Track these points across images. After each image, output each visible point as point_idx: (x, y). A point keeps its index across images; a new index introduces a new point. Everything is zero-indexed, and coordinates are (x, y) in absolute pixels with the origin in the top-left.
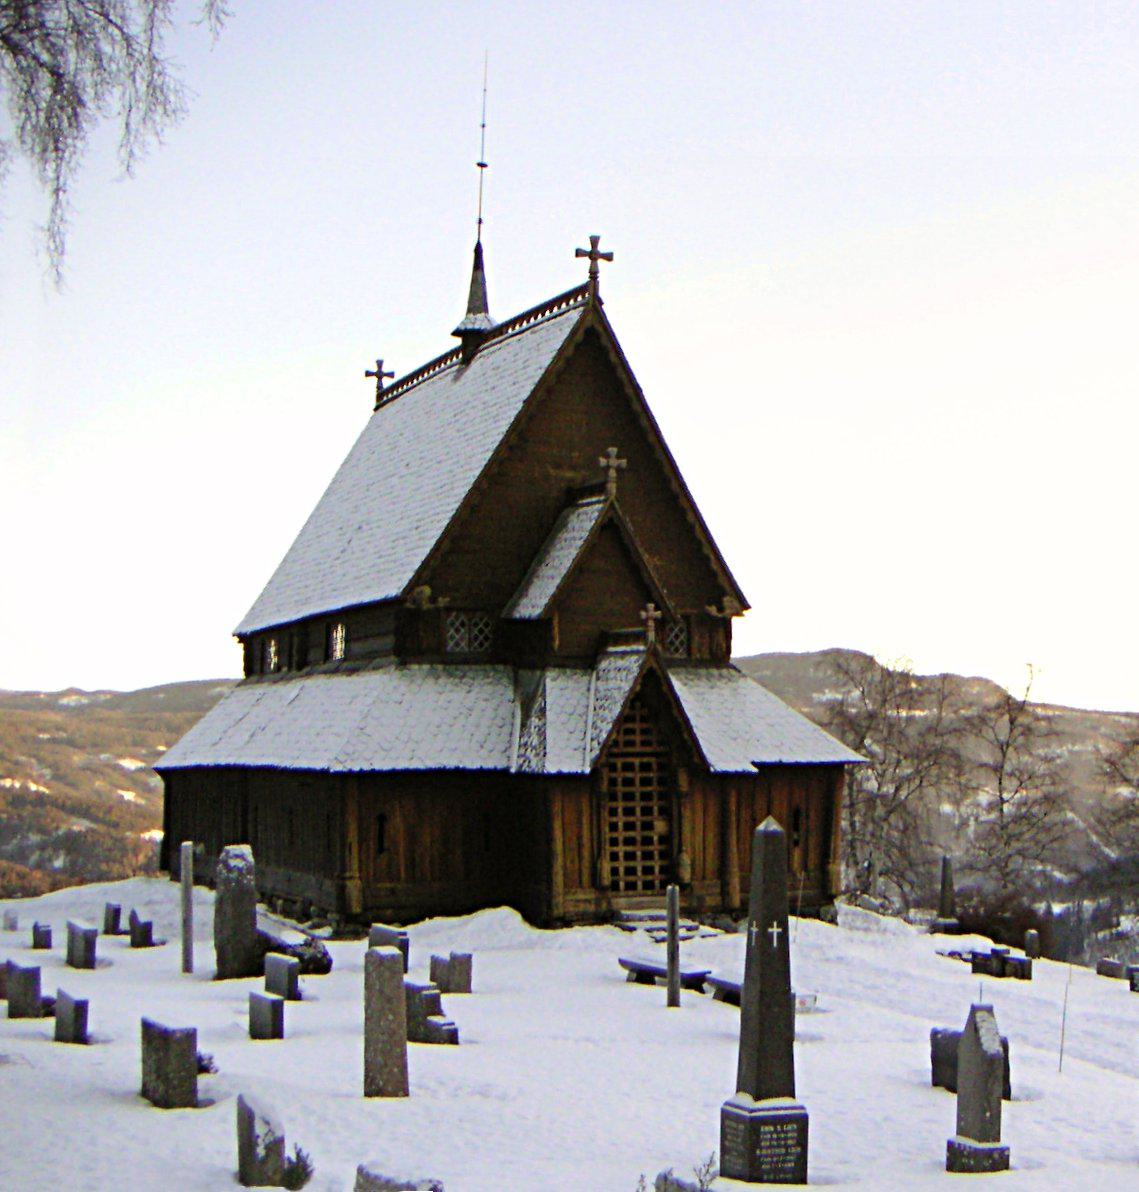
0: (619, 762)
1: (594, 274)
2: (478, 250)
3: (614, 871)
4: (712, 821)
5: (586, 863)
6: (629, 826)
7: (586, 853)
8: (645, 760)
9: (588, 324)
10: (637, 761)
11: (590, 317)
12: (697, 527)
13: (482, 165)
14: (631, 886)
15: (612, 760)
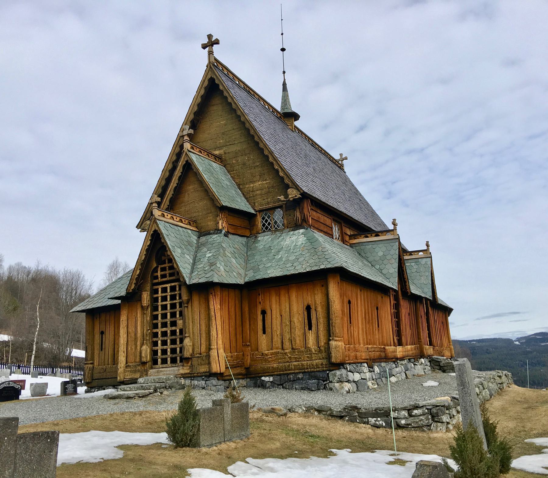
0: (160, 288)
1: (211, 53)
2: (284, 85)
3: (155, 353)
4: (203, 316)
5: (139, 348)
6: (164, 325)
7: (139, 343)
8: (173, 284)
9: (209, 77)
10: (168, 286)
11: (210, 73)
12: (270, 156)
13: (283, 50)
14: (164, 361)
15: (155, 287)
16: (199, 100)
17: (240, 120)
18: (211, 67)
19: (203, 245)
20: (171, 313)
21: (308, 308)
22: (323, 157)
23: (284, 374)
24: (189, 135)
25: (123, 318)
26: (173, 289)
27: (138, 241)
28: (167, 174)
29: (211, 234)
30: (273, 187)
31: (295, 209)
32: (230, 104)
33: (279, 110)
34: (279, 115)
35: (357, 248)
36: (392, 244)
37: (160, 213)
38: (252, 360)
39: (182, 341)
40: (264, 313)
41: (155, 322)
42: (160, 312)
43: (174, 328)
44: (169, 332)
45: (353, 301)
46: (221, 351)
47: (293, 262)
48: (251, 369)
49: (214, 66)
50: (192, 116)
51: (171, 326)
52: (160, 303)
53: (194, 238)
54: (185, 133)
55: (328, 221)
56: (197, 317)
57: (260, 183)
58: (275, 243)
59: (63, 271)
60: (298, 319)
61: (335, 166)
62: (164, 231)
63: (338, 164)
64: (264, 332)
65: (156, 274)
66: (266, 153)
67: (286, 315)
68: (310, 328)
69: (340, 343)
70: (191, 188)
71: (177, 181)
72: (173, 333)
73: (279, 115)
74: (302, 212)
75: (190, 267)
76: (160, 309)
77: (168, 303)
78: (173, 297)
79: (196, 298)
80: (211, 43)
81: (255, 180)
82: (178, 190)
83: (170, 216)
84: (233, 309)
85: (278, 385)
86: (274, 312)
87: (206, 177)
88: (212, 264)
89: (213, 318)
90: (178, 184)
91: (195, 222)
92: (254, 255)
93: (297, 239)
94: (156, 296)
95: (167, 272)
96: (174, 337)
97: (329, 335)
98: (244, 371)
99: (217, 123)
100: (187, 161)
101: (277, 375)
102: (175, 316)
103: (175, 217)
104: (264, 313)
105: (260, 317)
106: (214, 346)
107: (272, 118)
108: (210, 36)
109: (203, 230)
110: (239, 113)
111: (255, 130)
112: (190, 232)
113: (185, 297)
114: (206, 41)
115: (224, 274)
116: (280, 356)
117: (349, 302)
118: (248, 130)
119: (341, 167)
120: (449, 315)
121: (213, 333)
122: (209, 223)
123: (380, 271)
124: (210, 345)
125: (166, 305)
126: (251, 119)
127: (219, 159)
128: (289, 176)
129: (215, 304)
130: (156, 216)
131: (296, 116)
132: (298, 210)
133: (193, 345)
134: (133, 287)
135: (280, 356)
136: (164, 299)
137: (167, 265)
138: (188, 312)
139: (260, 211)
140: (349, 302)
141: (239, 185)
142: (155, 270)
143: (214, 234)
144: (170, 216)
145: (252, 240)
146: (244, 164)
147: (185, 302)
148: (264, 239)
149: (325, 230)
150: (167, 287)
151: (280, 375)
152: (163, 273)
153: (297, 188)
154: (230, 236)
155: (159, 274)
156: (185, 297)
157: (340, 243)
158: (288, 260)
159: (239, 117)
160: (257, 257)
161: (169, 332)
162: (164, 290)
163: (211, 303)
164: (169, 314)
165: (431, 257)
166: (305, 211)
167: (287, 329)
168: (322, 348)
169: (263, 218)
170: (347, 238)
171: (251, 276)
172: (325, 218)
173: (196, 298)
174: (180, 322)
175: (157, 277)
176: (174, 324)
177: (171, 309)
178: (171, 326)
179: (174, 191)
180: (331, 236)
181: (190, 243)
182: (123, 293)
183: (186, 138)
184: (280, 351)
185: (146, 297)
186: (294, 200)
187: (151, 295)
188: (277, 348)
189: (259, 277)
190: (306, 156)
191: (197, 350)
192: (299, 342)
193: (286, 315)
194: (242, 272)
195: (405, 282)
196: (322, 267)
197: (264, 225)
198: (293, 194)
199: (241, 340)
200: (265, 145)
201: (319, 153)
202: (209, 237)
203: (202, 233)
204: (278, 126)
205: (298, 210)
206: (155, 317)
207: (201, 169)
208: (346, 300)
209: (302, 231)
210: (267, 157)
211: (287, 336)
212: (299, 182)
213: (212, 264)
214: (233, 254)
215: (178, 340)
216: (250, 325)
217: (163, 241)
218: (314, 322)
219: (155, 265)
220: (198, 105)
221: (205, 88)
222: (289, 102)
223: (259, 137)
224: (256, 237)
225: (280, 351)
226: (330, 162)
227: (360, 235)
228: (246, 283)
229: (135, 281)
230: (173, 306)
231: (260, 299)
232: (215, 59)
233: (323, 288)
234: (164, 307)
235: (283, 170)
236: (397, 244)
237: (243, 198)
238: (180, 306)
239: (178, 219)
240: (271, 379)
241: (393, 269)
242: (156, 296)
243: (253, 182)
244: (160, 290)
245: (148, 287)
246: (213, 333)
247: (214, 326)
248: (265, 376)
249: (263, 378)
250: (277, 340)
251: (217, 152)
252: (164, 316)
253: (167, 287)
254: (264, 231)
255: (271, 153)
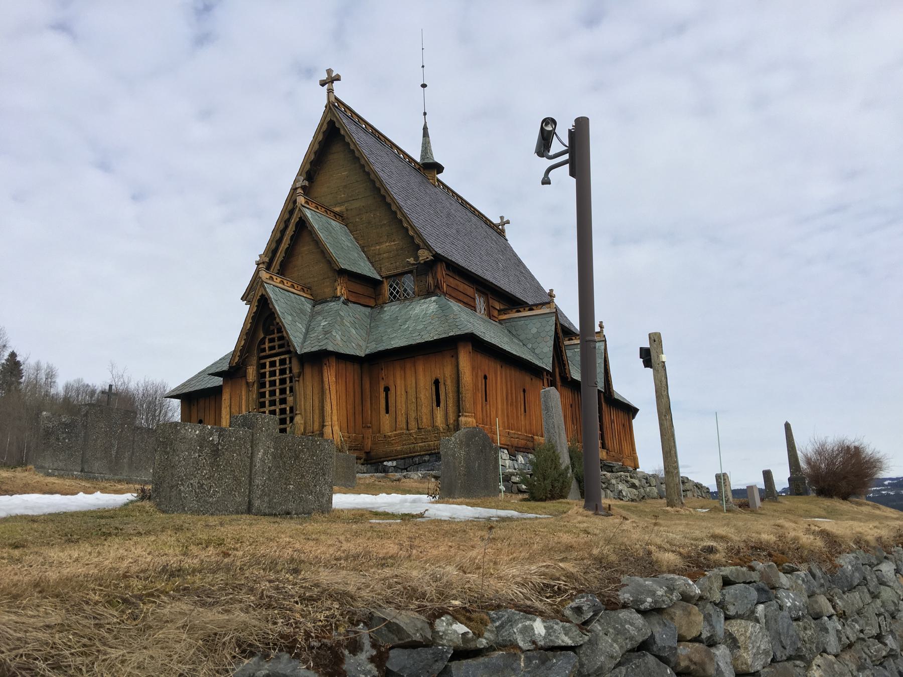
0: (267, 362)
1: (330, 91)
2: (425, 129)
4: (316, 391)
6: (273, 403)
8: (283, 357)
9: (328, 119)
10: (277, 359)
13: (424, 86)
15: (263, 361)
16: (317, 147)
17: (364, 171)
18: (330, 108)
19: (318, 313)
20: (280, 390)
21: (437, 383)
22: (474, 219)
23: (409, 457)
24: (303, 188)
25: (226, 396)
26: (283, 362)
27: (241, 312)
28: (278, 235)
29: (326, 301)
30: (402, 249)
31: (427, 274)
32: (353, 151)
33: (419, 160)
34: (417, 167)
35: (508, 324)
36: (548, 319)
37: (268, 276)
38: (374, 443)
39: (292, 419)
40: (387, 389)
41: (262, 400)
42: (268, 388)
43: (283, 406)
44: (278, 410)
45: (491, 377)
46: (336, 428)
47: (420, 331)
48: (372, 454)
49: (335, 107)
50: (308, 167)
51: (280, 404)
52: (268, 379)
53: (308, 307)
54: (298, 185)
55: (470, 290)
56: (309, 392)
57: (388, 246)
58: (403, 312)
59: (142, 382)
60: (426, 394)
61: (492, 230)
62: (271, 296)
63: (498, 230)
64: (387, 412)
65: (263, 346)
66: (394, 208)
67: (412, 392)
68: (438, 405)
69: (470, 419)
70: (305, 250)
71: (288, 242)
72: (283, 411)
73: (417, 167)
74: (435, 277)
75: (302, 337)
76: (267, 386)
77: (277, 378)
78: (283, 372)
79: (308, 371)
80: (330, 80)
81: (381, 240)
82: (290, 252)
83: (279, 279)
84: (351, 385)
85: (402, 469)
86: (398, 389)
87: (322, 235)
88: (326, 333)
89: (328, 392)
90: (290, 245)
91: (309, 288)
92: (377, 327)
93: (430, 306)
94: (263, 371)
95: (276, 343)
96: (283, 416)
97: (459, 411)
98: (364, 456)
99: (337, 174)
100: (300, 218)
101: (401, 459)
102: (285, 393)
103: (285, 282)
104: (387, 389)
105: (383, 395)
106: (328, 423)
107: (408, 169)
108: (329, 71)
109: (319, 298)
110: (363, 162)
111: (381, 182)
112: (303, 299)
113: (296, 370)
114: (324, 77)
115: (340, 343)
116: (404, 437)
117: (485, 377)
118: (373, 182)
119: (501, 233)
120: (633, 418)
121: (328, 408)
122: (326, 290)
123: (533, 350)
124: (323, 422)
125: (275, 381)
126: (377, 169)
127: (339, 216)
128: (419, 235)
129: (330, 375)
130: (264, 279)
131: (439, 168)
132: (430, 275)
133: (305, 423)
134: (236, 360)
135: (404, 437)
136: (273, 374)
137: (276, 336)
138: (299, 387)
139: (387, 278)
140: (485, 377)
141: (363, 248)
142: (263, 342)
143: (331, 301)
144: (279, 279)
145: (376, 311)
146: (369, 223)
147: (296, 375)
148: (391, 310)
149: (465, 300)
150: (275, 361)
151: (404, 458)
152: (271, 344)
153: (429, 248)
154: (350, 305)
155: (267, 345)
156: (296, 370)
157: (487, 318)
158: (415, 330)
159: (363, 166)
160: (381, 329)
161: (278, 410)
162: (273, 364)
163: (325, 375)
164: (278, 391)
165: (605, 341)
166: (439, 276)
167: (413, 407)
168: (451, 426)
169: (391, 286)
170: (496, 313)
171: (373, 348)
172: (466, 287)
173: (308, 371)
174: (290, 399)
175: (264, 350)
176: (283, 401)
177: (280, 384)
178: (280, 404)
179: (286, 253)
180: (474, 308)
181: (302, 312)
182: (225, 367)
183: (299, 191)
184: (405, 431)
185: (251, 373)
186: (425, 262)
187: (258, 371)
188: (401, 429)
189: (382, 347)
190: (449, 215)
191: (309, 429)
192: (425, 421)
193: (412, 392)
194: (362, 343)
195: (564, 365)
196: (451, 334)
197: (391, 294)
198: (424, 255)
199: (360, 419)
200: (393, 199)
201: (469, 214)
202: (325, 305)
203: (317, 301)
204: (415, 179)
205: (430, 275)
206: (263, 395)
207: (316, 227)
208: (481, 375)
209: (434, 298)
210: (395, 213)
211: (413, 415)
212: (431, 242)
213: (326, 333)
214: (353, 324)
215: (288, 419)
216: (371, 404)
217: (271, 306)
218: (442, 397)
219: (262, 336)
220: (315, 153)
221: (324, 132)
222: (430, 150)
223: (386, 191)
224: (382, 307)
225: (405, 431)
226: (484, 225)
227: (511, 309)
228: (367, 355)
229: (239, 354)
230: (283, 381)
231: (383, 373)
232: (336, 98)
233: (454, 359)
234: (273, 383)
235: (413, 228)
236: (554, 318)
237: (368, 263)
238: (291, 381)
239: (290, 284)
240: (395, 463)
241: (547, 348)
242: (263, 371)
243: (381, 243)
244: (268, 364)
245: (254, 360)
246: (328, 407)
247: (328, 400)
248: (388, 461)
249: (385, 463)
250: (401, 419)
251: (337, 209)
252: (273, 393)
253: (275, 361)
254: (392, 301)
255: (400, 208)
